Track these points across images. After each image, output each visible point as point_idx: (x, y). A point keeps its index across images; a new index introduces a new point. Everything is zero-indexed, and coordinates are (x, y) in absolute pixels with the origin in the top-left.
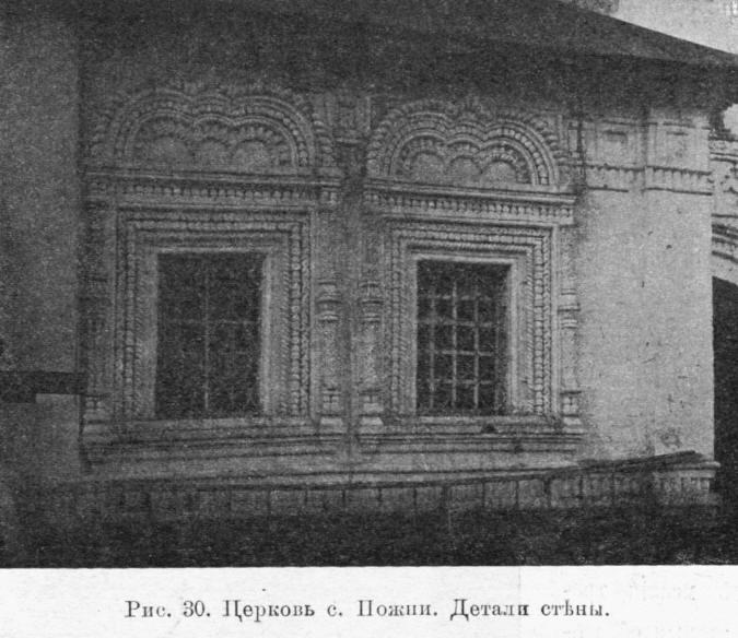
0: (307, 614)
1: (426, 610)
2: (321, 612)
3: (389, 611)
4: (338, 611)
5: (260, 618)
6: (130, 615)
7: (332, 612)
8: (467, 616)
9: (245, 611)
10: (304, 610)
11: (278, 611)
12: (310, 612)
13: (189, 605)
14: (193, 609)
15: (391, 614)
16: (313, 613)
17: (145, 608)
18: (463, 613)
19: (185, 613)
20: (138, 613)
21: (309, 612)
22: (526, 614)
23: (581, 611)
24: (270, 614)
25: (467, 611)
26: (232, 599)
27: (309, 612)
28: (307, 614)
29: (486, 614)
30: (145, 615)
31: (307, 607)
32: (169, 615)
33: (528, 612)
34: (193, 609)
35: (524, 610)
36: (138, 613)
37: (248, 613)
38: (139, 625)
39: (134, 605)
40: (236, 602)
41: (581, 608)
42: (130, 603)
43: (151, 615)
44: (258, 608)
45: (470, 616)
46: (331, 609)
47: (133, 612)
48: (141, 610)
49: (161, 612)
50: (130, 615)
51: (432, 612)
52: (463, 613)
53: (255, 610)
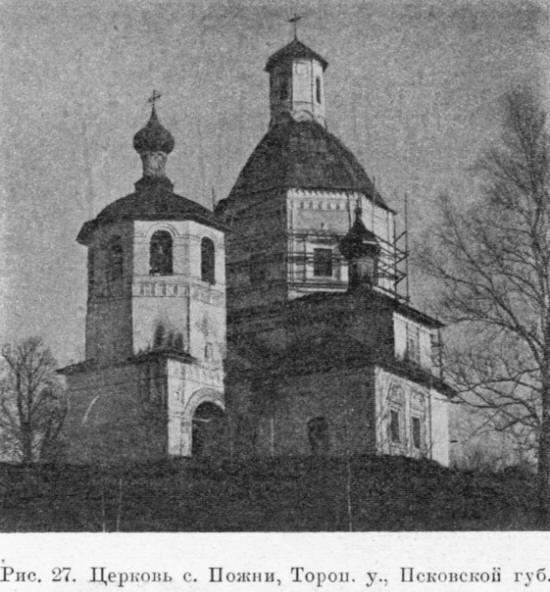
0: (165, 580)
1: (270, 577)
2: (177, 576)
4: (193, 577)
5: (123, 584)
6: (5, 580)
7: (188, 577)
8: (106, 582)
9: (109, 577)
10: (162, 577)
13: (57, 571)
15: (239, 580)
16: (171, 579)
17: (18, 574)
18: (102, 580)
19: (34, 575)
21: (167, 578)
23: (257, 577)
24: (132, 580)
25: (106, 578)
26: (216, 565)
27: (167, 578)
28: (165, 580)
30: (18, 580)
31: (165, 574)
32: (195, 580)
36: (12, 578)
43: (23, 580)
45: (108, 582)
46: (187, 576)
48: (14, 576)
49: (32, 577)
50: (5, 580)
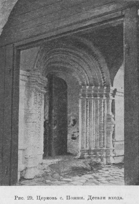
0: (55, 199)
1: (82, 198)
2: (58, 198)
3: (73, 198)
8: (40, 200)
9: (41, 198)
10: (55, 198)
11: (49, 198)
12: (56, 199)
13: (29, 197)
14: (30, 198)
15: (74, 199)
16: (57, 199)
18: (39, 199)
19: (23, 198)
20: (17, 199)
22: (105, 199)
23: (78, 198)
24: (47, 199)
25: (40, 199)
27: (56, 199)
28: (55, 199)
29: (96, 199)
30: (19, 199)
31: (55, 197)
32: (63, 199)
33: (105, 199)
34: (30, 198)
35: (109, 198)
36: (17, 199)
37: (42, 199)
38: (18, 201)
39: (16, 197)
40: (39, 196)
41: (78, 198)
42: (16, 196)
43: (20, 199)
44: (44, 198)
45: (41, 200)
46: (61, 198)
47: (16, 199)
48: (18, 198)
49: (22, 199)
50: (16, 199)
51: (83, 198)
52: (39, 199)
53: (44, 198)
